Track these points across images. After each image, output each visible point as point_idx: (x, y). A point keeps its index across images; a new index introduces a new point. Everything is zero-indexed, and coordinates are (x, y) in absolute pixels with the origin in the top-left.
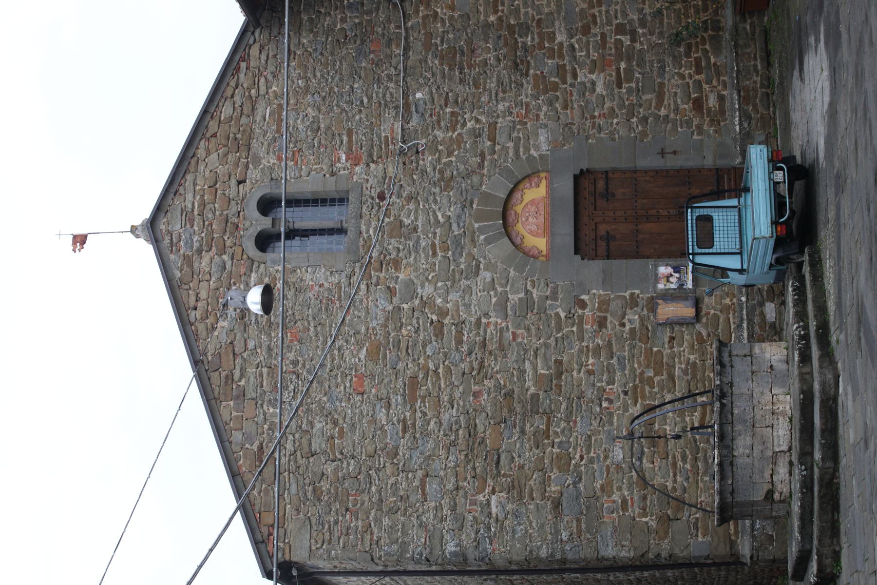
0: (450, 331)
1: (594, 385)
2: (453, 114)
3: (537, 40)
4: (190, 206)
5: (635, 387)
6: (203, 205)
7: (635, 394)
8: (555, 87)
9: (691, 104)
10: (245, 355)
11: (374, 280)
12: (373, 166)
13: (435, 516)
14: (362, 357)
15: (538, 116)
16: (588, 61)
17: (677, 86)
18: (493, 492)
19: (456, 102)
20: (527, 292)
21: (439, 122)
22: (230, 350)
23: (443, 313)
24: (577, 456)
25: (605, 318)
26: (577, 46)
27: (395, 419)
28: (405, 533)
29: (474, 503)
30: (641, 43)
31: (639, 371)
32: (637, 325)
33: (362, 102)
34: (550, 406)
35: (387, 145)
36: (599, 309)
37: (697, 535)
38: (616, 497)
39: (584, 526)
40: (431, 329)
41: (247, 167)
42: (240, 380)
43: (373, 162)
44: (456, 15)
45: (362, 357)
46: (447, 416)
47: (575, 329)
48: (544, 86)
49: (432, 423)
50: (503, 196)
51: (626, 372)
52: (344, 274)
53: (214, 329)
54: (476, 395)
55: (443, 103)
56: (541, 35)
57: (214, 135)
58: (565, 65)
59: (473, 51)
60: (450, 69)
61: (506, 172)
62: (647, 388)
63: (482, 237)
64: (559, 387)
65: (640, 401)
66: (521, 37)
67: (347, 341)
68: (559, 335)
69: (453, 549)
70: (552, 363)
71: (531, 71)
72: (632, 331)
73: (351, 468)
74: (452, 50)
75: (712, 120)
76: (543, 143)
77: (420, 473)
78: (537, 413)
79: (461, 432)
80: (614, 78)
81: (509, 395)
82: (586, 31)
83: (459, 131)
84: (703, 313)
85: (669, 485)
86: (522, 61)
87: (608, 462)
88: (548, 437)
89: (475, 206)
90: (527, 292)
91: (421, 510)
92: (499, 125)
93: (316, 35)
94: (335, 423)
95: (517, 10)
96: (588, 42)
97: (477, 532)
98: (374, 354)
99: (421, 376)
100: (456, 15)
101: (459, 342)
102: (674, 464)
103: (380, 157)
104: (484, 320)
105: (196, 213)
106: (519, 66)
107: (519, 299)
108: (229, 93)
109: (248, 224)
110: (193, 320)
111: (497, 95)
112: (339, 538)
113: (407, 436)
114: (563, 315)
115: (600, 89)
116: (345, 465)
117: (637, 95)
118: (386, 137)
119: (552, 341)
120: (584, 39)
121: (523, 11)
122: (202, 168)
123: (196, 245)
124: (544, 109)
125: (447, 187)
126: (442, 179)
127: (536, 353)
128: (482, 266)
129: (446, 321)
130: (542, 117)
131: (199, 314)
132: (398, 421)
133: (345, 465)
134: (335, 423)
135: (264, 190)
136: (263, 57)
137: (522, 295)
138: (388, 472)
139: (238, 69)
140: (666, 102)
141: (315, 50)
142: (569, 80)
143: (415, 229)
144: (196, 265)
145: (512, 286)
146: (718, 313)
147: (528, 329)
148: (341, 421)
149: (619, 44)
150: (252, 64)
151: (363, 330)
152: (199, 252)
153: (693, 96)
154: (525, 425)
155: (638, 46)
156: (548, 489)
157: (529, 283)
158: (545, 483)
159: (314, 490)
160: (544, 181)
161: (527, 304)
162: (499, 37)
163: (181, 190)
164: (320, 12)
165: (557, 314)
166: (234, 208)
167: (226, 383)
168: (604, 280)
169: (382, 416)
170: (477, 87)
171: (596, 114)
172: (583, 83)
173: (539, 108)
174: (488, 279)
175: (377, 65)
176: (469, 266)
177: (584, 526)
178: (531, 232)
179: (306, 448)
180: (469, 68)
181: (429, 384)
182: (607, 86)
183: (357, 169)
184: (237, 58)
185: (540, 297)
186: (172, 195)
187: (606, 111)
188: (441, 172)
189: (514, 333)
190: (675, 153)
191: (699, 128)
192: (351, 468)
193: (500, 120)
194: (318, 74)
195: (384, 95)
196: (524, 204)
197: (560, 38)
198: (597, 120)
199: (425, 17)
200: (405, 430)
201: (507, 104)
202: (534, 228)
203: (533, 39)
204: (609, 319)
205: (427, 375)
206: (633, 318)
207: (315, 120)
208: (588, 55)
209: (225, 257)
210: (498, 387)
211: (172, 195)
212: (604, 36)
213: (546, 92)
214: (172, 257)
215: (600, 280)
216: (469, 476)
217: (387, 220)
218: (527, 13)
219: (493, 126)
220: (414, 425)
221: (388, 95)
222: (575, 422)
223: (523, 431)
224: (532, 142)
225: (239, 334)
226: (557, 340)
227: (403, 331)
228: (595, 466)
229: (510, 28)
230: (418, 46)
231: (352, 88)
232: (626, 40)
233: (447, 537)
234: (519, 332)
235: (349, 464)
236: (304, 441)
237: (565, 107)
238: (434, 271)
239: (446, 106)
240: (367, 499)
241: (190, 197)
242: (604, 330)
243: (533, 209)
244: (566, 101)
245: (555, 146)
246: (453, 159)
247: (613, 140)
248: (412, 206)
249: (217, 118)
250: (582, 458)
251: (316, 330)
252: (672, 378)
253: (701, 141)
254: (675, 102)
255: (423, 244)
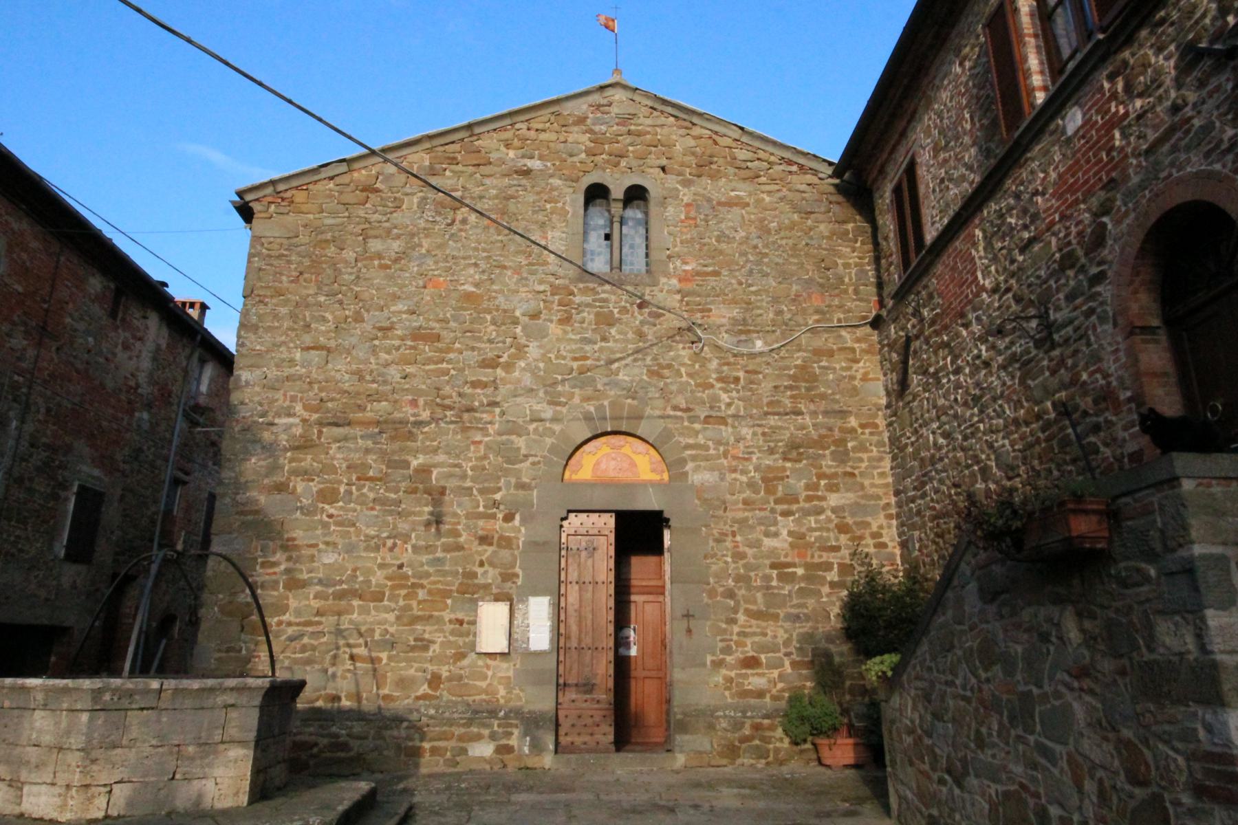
0: (485, 375)
1: (414, 530)
2: (737, 380)
3: (828, 471)
4: (639, 121)
5: (406, 577)
6: (639, 134)
7: (398, 576)
8: (770, 491)
9: (751, 654)
10: (478, 175)
11: (550, 298)
12: (678, 297)
13: (283, 360)
14: (466, 287)
15: (735, 471)
16: (803, 530)
17: (775, 637)
18: (304, 421)
19: (752, 382)
20: (526, 456)
21: (728, 364)
22: (482, 162)
23: (509, 367)
24: (332, 511)
25: (491, 544)
26: (822, 517)
27: (395, 319)
28: (269, 329)
29: (293, 399)
30: (828, 595)
31: (425, 582)
32: (480, 580)
33: (750, 285)
34: (394, 481)
35: (702, 311)
36: (501, 538)
37: (219, 651)
38: (279, 556)
39: (250, 518)
40: (490, 355)
41: (679, 174)
42: (452, 171)
43: (683, 297)
44: (856, 383)
45: (466, 287)
46: (393, 372)
47: (481, 509)
48: (771, 479)
49: (387, 357)
50: (639, 433)
51: (426, 568)
52: (556, 268)
53: (508, 146)
54: (414, 403)
55: (750, 368)
56: (835, 475)
57: (716, 143)
58: (798, 502)
59: (812, 401)
60: (789, 376)
61: (667, 435)
62: (403, 592)
63: (592, 409)
64: (414, 491)
65: (389, 583)
66: (832, 453)
67: (483, 272)
68: (475, 492)
69: (243, 379)
70: (442, 483)
71: (788, 465)
72: (475, 575)
73: (346, 277)
74: (813, 378)
75: (730, 680)
76: (700, 477)
77: (332, 344)
78: (388, 467)
79: (375, 385)
80: (782, 559)
81: (411, 436)
82: (842, 528)
83: (719, 385)
84: (489, 662)
85: (286, 618)
86: (801, 454)
87: (322, 546)
88: (359, 479)
89: (629, 401)
90: (526, 456)
91: (292, 345)
92: (723, 427)
93: (829, 238)
94: (396, 261)
95: (866, 450)
96: (828, 530)
97: (261, 404)
98: (468, 296)
99: (440, 345)
100: (856, 383)
101: (474, 385)
102: (308, 623)
103: (687, 304)
104: (497, 410)
105: (633, 128)
106: (795, 450)
107: (519, 449)
108: (761, 154)
109: (617, 176)
110: (517, 126)
111: (759, 426)
112: (271, 265)
113: (375, 331)
114: (498, 496)
115: (768, 543)
116: (349, 270)
117: (762, 587)
118: (710, 310)
119: (468, 484)
120: (832, 526)
121: (865, 456)
122: (683, 131)
123: (597, 128)
124: (744, 479)
125: (651, 373)
126: (661, 367)
127: (456, 466)
128: (558, 408)
129: (499, 371)
130: (734, 475)
131: (524, 132)
132: (393, 323)
133: (349, 270)
134: (396, 261)
135: (654, 191)
136: (803, 187)
137: (523, 451)
138: (337, 313)
139: (790, 163)
140: (754, 622)
141: (811, 238)
142: (779, 508)
143: (604, 339)
144: (576, 129)
145: (534, 441)
146: (488, 681)
147: (485, 457)
148: (397, 266)
149: (828, 567)
150: (795, 177)
151: (495, 287)
152: (591, 131)
153: (763, 656)
154: (375, 453)
155: (826, 590)
156: (299, 479)
157: (536, 459)
158: (307, 475)
159: (327, 241)
160: (658, 477)
161: (512, 456)
162: (830, 429)
163: (655, 113)
164: (856, 242)
165: (499, 489)
166: (634, 163)
167: (449, 158)
168: (536, 544)
169: (400, 306)
170: (770, 404)
171: (738, 538)
172: (775, 523)
173: (744, 472)
174: (543, 416)
175: (794, 300)
176: (560, 394)
177: (250, 518)
178: (598, 463)
179: (371, 232)
180: (791, 397)
181: (430, 354)
182: (773, 552)
183: (674, 281)
184: (802, 161)
185: (520, 471)
186: (650, 103)
187: (741, 549)
188: (669, 366)
189: (480, 442)
190: (689, 631)
191: (718, 664)
192: (346, 277)
193: (730, 430)
194: (784, 242)
195: (759, 308)
196: (633, 456)
197: (834, 500)
198: (730, 538)
199: (853, 350)
200: (381, 329)
201: (749, 437)
202: (603, 466)
203: (830, 467)
204: (490, 549)
205: (441, 351)
206: (489, 575)
207: (730, 240)
208: (811, 530)
209: (583, 155)
210: (419, 424)
211: (650, 103)
212: (836, 549)
213: (764, 479)
214: (585, 107)
215: (538, 539)
216: (323, 394)
217: (616, 311)
218: (861, 460)
219: (722, 421)
220: (385, 337)
221: (759, 312)
222: (372, 509)
223: (367, 451)
224: (702, 464)
225: (499, 169)
226: (470, 489)
227: (493, 327)
228: (319, 532)
229: (842, 442)
230: (819, 342)
231: (767, 275)
232: (833, 576)
233: (258, 372)
234: (482, 447)
235: (351, 274)
236: (380, 232)
237: (745, 502)
238: (557, 358)
239: (747, 372)
240: (311, 292)
241: (649, 121)
242: (477, 542)
243: (625, 465)
244: (753, 503)
245: (699, 491)
246: (685, 378)
247: (706, 557)
248: (630, 335)
249: (734, 145)
250: (330, 516)
251: (497, 241)
252: (416, 620)
253: (704, 665)
254: (754, 634)
255: (588, 348)
